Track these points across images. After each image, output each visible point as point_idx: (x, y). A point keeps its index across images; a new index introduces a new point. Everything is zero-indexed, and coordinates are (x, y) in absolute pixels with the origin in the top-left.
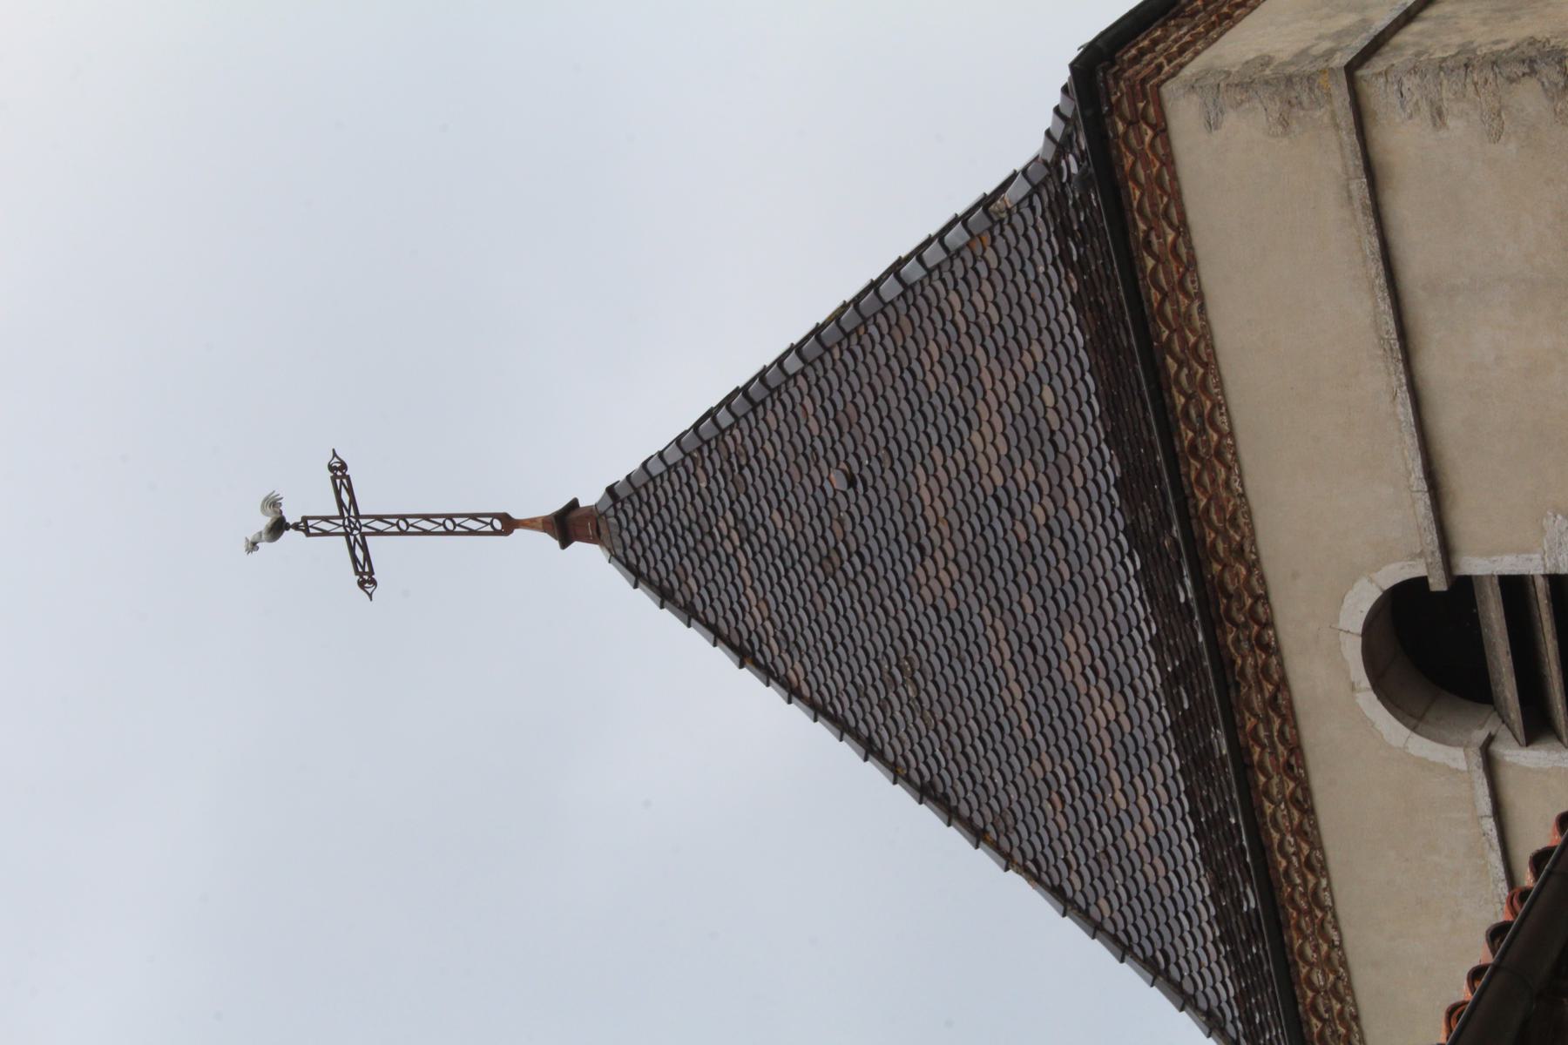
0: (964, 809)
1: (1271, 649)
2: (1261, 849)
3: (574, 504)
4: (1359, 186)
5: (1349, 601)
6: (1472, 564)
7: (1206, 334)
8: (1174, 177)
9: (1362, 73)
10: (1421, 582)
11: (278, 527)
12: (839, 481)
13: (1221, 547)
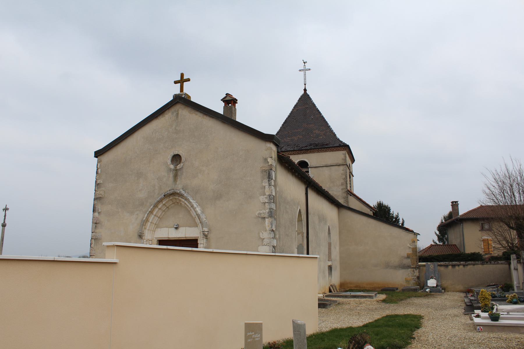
1: (303, 154)
2: (286, 151)
4: (338, 164)
5: (307, 160)
6: (310, 169)
7: (327, 152)
12: (312, 117)
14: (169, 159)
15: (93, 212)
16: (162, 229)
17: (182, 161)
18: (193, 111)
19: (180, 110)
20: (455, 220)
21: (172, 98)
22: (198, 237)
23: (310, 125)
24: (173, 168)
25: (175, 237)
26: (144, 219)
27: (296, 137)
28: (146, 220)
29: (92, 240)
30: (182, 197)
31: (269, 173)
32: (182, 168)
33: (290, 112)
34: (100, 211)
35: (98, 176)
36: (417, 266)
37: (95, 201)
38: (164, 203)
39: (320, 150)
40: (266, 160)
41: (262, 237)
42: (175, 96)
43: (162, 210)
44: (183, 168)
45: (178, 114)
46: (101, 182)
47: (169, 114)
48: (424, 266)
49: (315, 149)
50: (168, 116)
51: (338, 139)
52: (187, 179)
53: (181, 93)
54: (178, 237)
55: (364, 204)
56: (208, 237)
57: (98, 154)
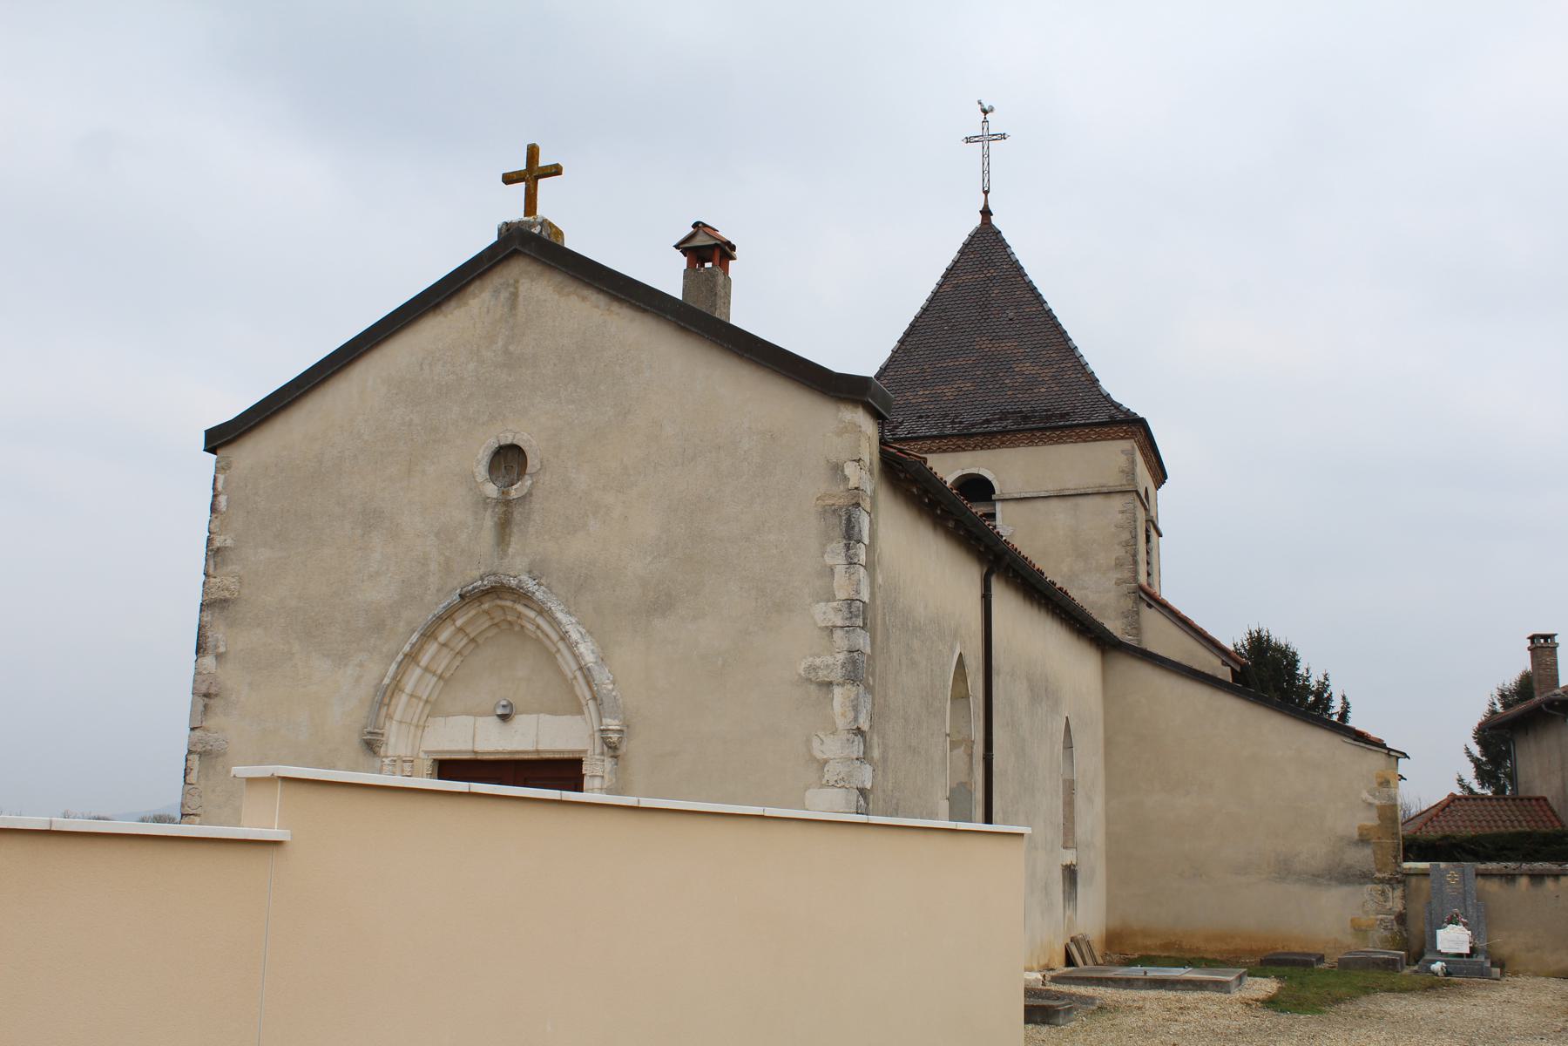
0: (909, 339)
1: (974, 449)
3: (992, 215)
4: (1105, 490)
6: (999, 506)
7: (1065, 442)
8: (1109, 439)
9: (1135, 494)
10: (994, 493)
11: (985, 112)
12: (1011, 315)
13: (1005, 439)
14: (479, 462)
15: (197, 652)
16: (451, 718)
17: (528, 471)
18: (571, 286)
19: (522, 281)
20: (1543, 706)
21: (493, 238)
22: (585, 751)
23: (1002, 345)
24: (495, 496)
25: (500, 749)
26: (386, 681)
27: (950, 386)
28: (392, 686)
29: (189, 757)
30: (526, 602)
31: (849, 520)
32: (530, 494)
33: (928, 294)
34: (222, 649)
35: (217, 522)
36: (1398, 873)
37: (205, 614)
38: (459, 623)
39: (1038, 438)
40: (837, 470)
41: (819, 755)
42: (504, 230)
43: (452, 650)
44: (531, 495)
45: (514, 296)
46: (229, 543)
47: (483, 295)
48: (1424, 874)
49: (1019, 431)
50: (479, 302)
51: (1104, 397)
52: (546, 537)
53: (526, 219)
54: (509, 748)
55: (1198, 638)
56: (619, 753)
57: (218, 439)
